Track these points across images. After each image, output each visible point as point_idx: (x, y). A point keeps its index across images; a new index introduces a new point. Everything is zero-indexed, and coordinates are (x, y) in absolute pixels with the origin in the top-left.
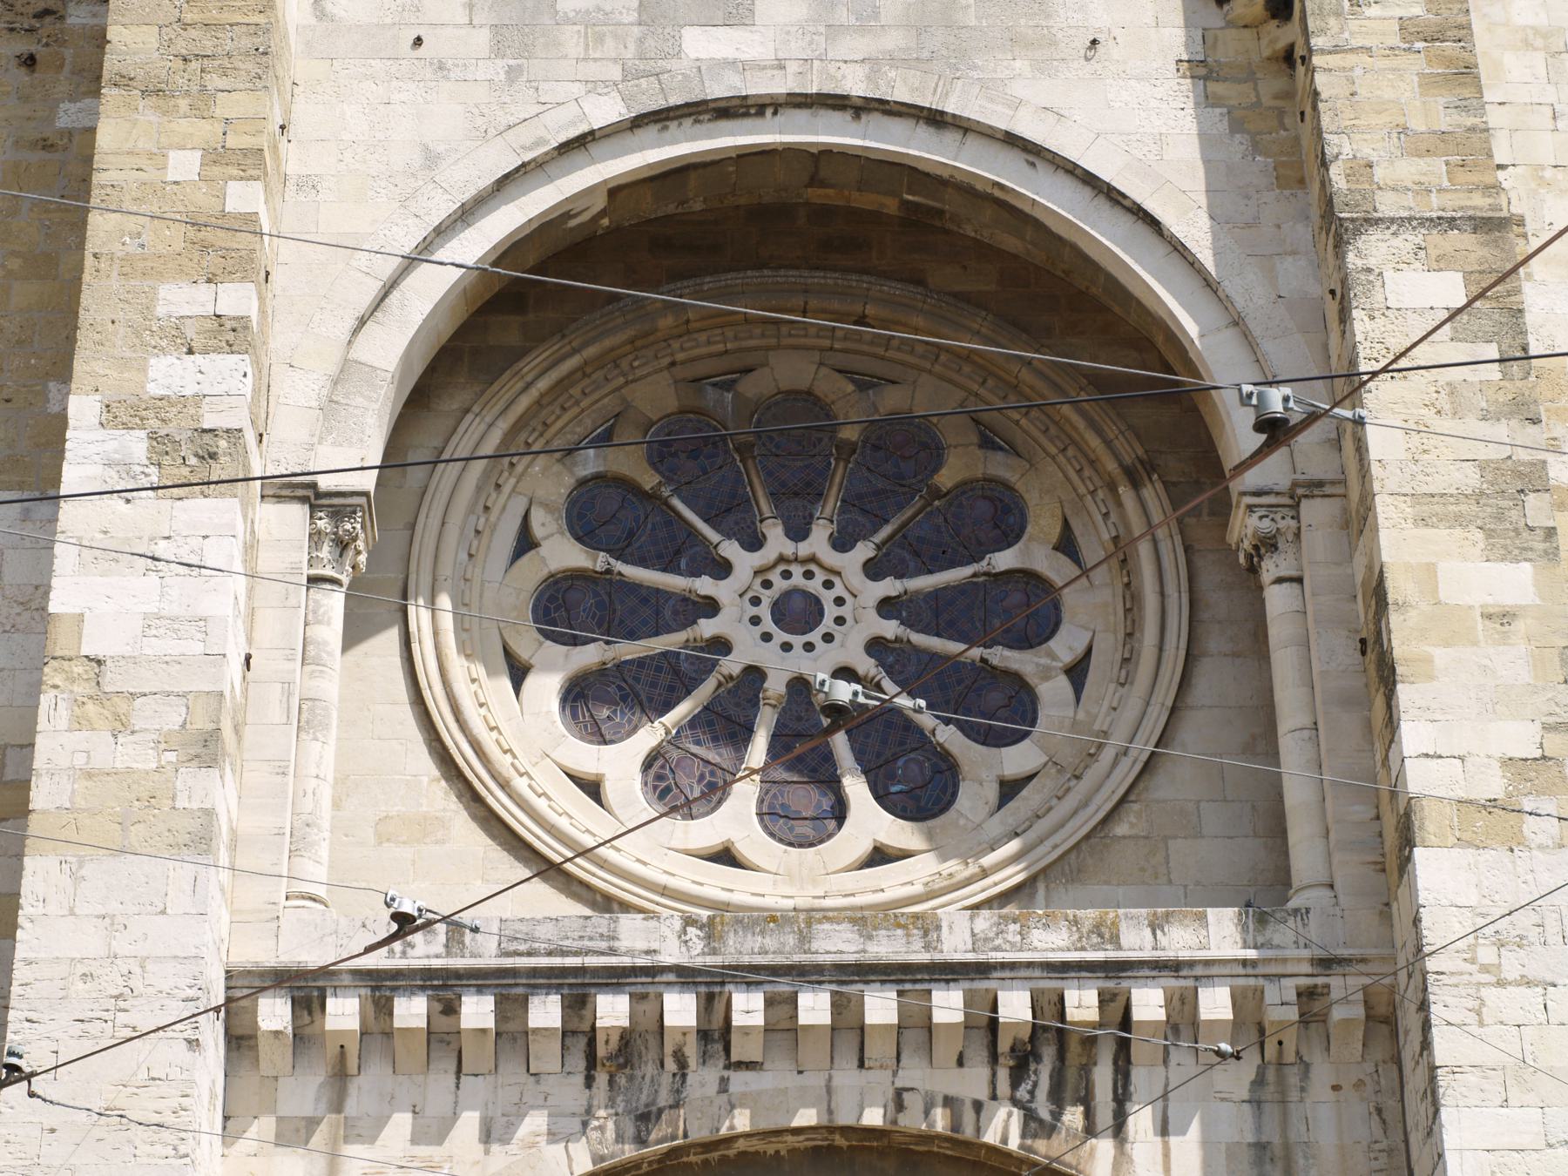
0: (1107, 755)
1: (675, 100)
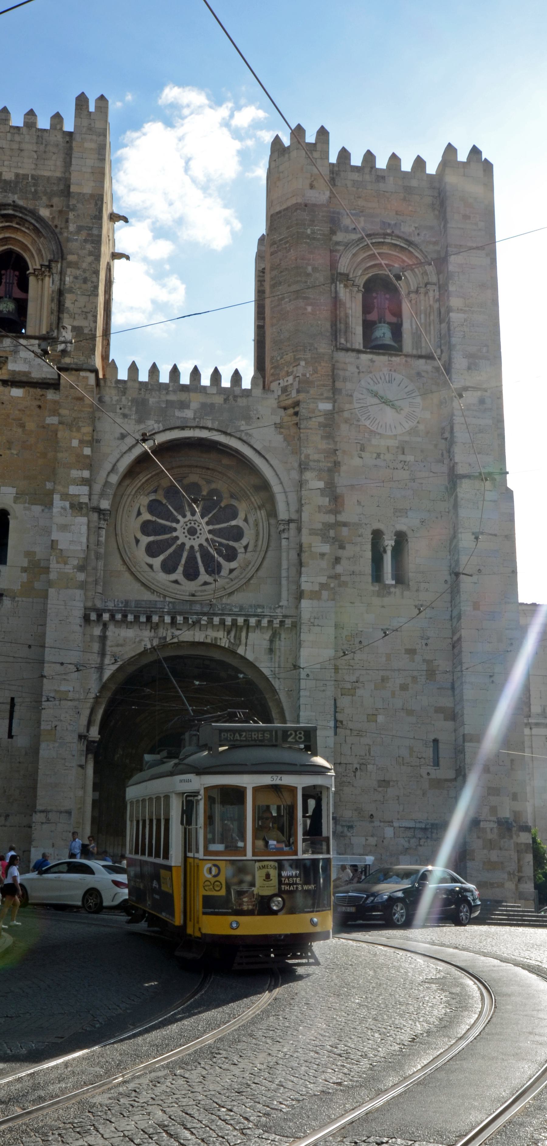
0: (250, 567)
1: (173, 426)
